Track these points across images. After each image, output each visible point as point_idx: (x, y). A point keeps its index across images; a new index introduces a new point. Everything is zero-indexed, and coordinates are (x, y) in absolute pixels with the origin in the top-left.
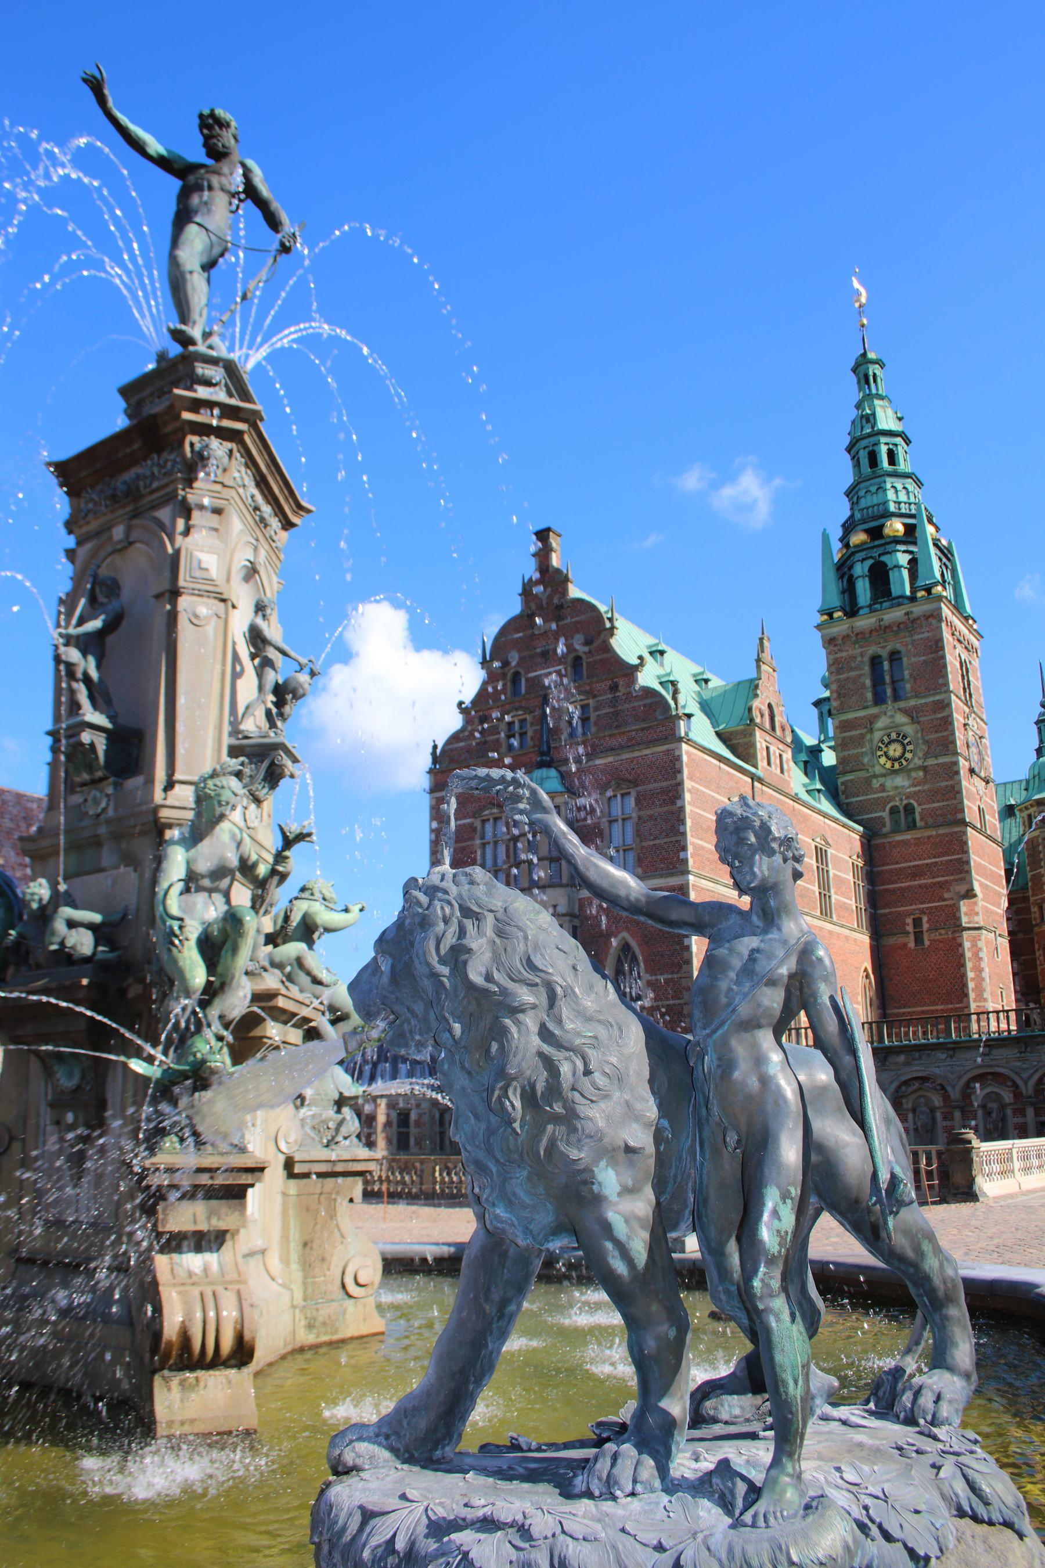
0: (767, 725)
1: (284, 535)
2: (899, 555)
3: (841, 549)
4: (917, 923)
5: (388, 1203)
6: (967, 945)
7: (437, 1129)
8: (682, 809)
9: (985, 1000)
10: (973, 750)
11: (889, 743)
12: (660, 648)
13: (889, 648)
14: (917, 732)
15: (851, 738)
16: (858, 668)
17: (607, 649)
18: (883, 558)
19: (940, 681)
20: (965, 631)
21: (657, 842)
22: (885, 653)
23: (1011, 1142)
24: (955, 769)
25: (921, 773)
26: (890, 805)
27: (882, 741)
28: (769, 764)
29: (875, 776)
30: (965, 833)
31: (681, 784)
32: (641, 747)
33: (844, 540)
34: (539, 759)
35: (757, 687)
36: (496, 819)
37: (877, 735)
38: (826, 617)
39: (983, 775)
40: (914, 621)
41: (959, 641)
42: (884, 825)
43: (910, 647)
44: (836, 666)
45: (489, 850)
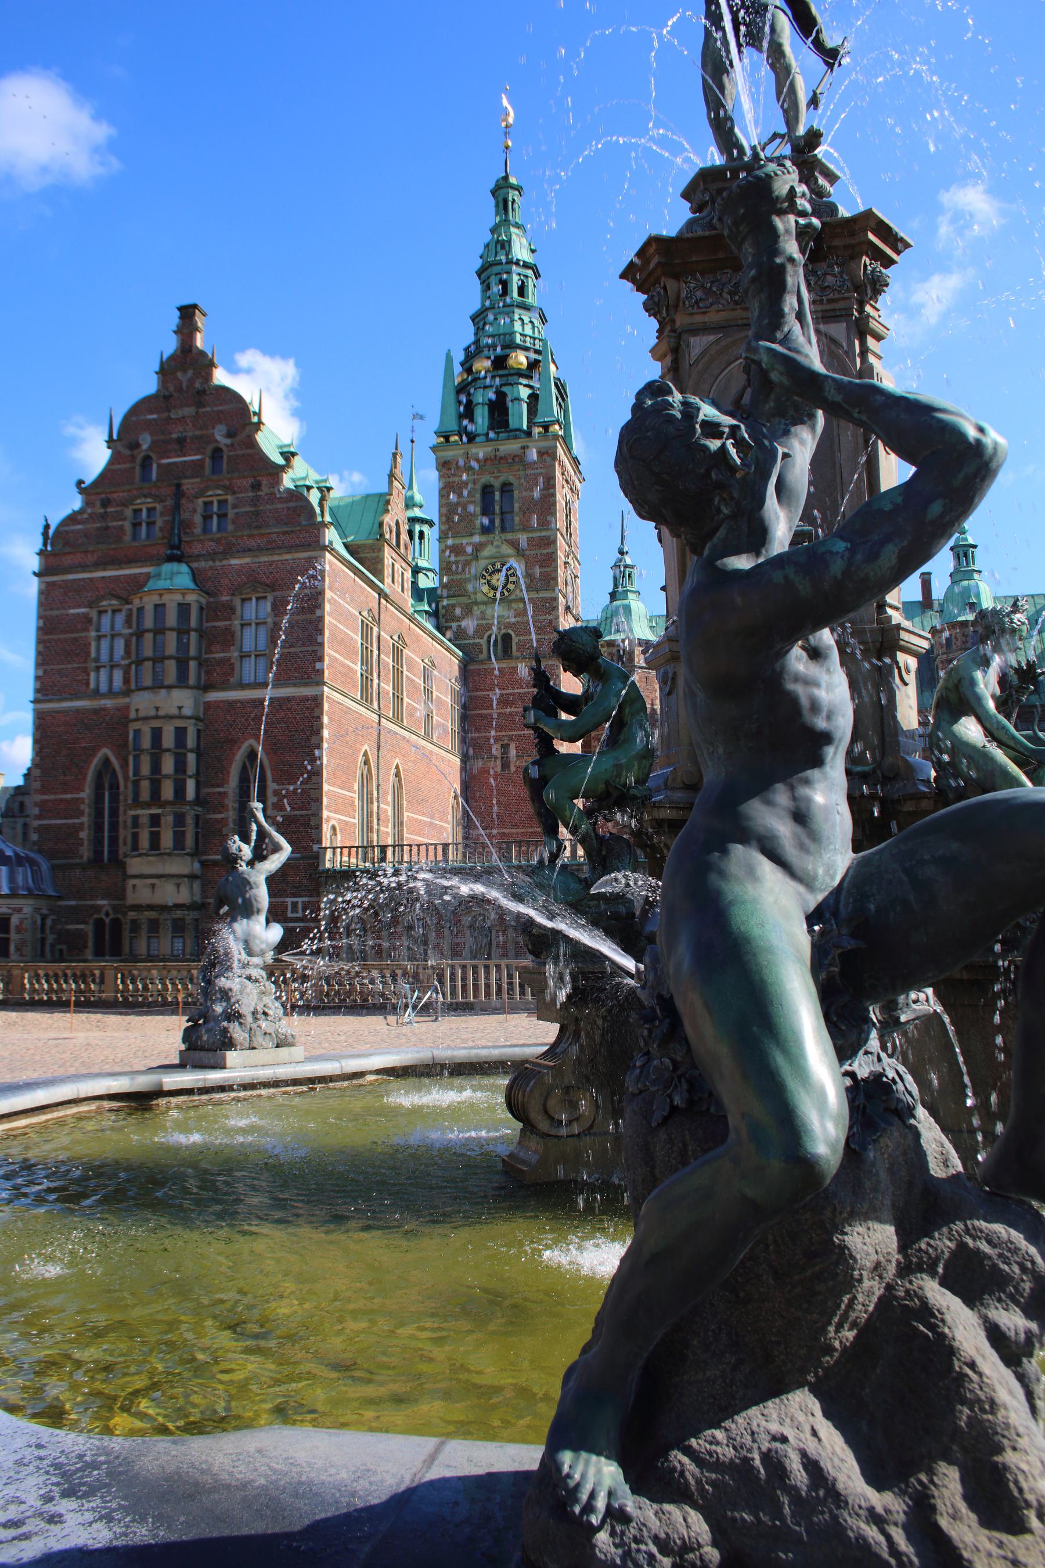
0: (394, 542)
2: (521, 388)
3: (461, 374)
5: (75, 1012)
7: (39, 936)
8: (321, 619)
10: (570, 588)
11: (493, 572)
13: (502, 479)
17: (253, 445)
18: (505, 389)
21: (292, 650)
22: (497, 484)
27: (486, 570)
28: (393, 582)
29: (476, 603)
32: (281, 551)
33: (467, 366)
34: (169, 552)
35: (388, 502)
36: (114, 611)
37: (483, 563)
38: (442, 439)
41: (567, 481)
42: (481, 652)
43: (522, 480)
45: (105, 644)
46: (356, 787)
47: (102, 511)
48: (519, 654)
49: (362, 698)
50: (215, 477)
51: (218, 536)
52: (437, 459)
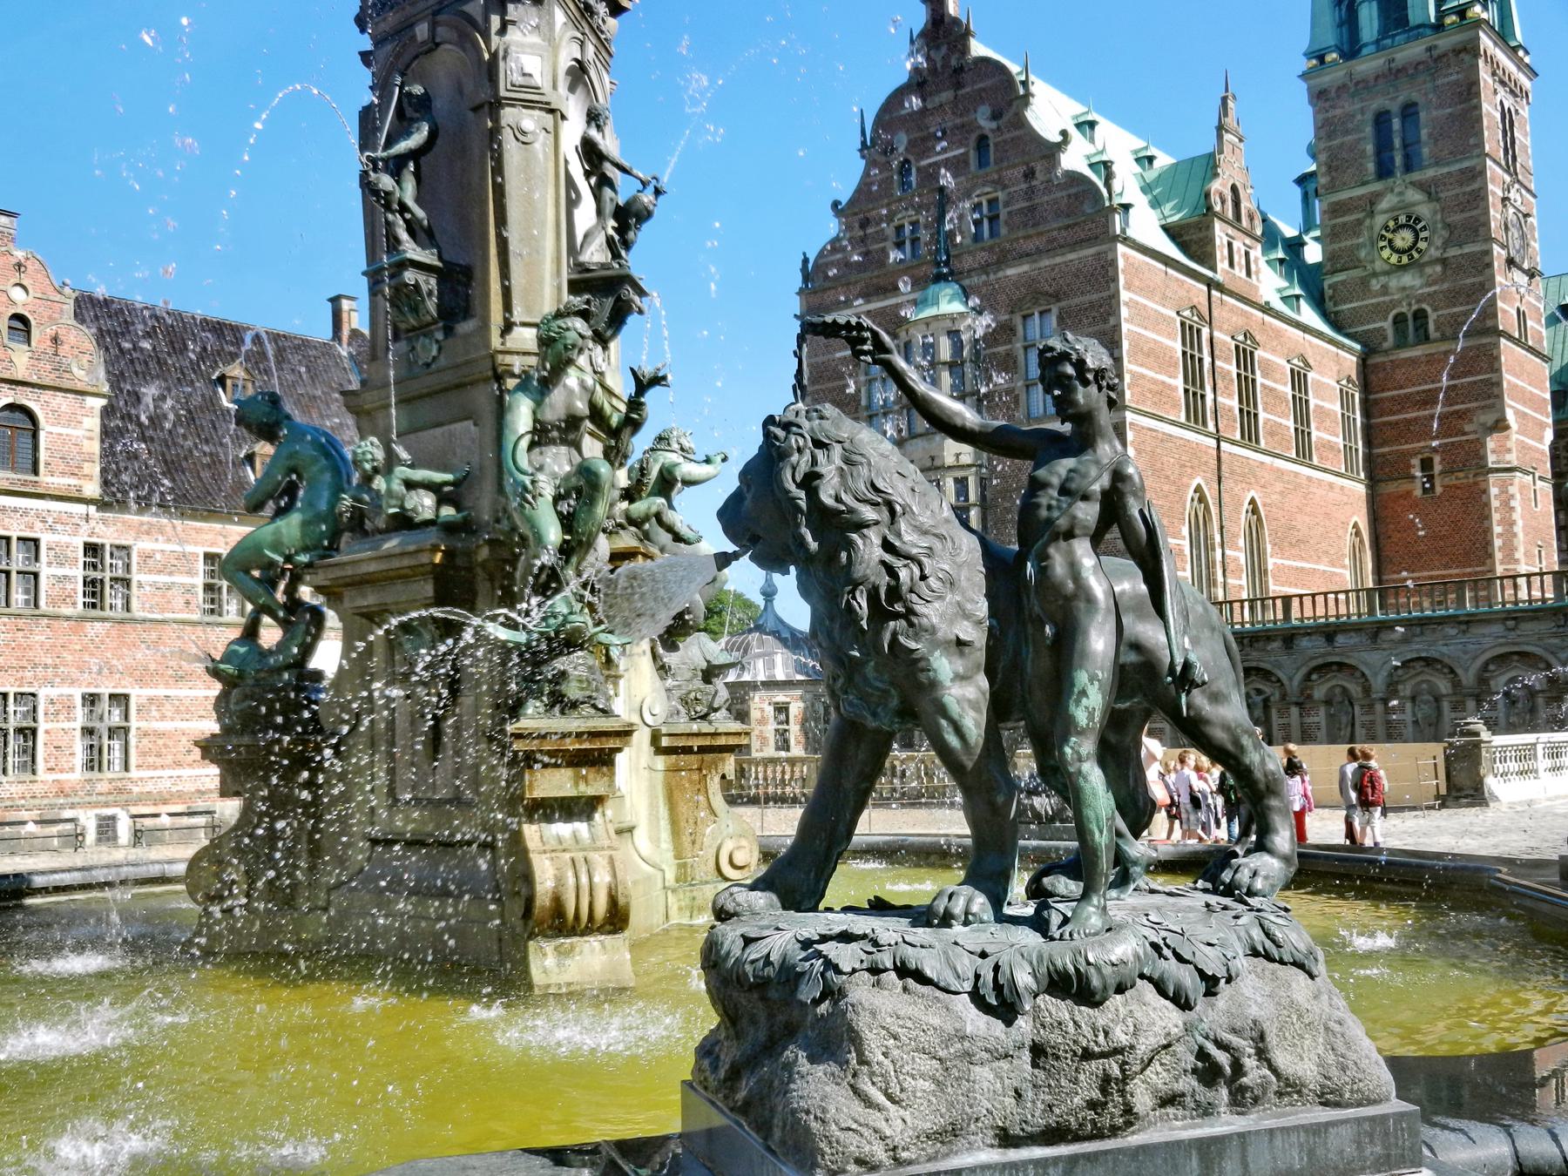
0: (1230, 214)
1: (612, 23)
4: (1427, 465)
6: (1494, 491)
9: (1517, 561)
10: (1514, 232)
11: (1394, 231)
12: (1090, 118)
13: (1401, 99)
14: (1435, 213)
15: (1345, 224)
16: (1358, 129)
17: (1021, 123)
19: (1472, 141)
20: (1511, 67)
23: (1534, 736)
24: (1487, 260)
25: (1438, 268)
26: (1394, 312)
27: (1386, 228)
28: (1231, 264)
30: (1497, 345)
31: (1115, 296)
35: (1216, 166)
37: (1380, 220)
38: (1314, 62)
39: (1526, 266)
40: (1440, 57)
42: (1385, 339)
44: (1327, 129)
46: (1185, 531)
47: (861, 233)
48: (1438, 335)
49: (1188, 418)
50: (982, 172)
51: (991, 242)
52: (1309, 89)
